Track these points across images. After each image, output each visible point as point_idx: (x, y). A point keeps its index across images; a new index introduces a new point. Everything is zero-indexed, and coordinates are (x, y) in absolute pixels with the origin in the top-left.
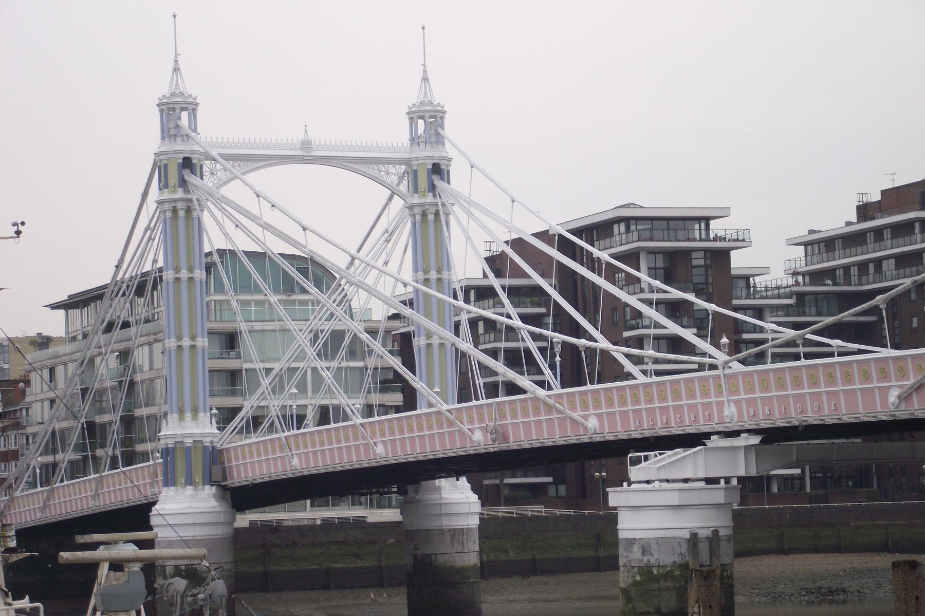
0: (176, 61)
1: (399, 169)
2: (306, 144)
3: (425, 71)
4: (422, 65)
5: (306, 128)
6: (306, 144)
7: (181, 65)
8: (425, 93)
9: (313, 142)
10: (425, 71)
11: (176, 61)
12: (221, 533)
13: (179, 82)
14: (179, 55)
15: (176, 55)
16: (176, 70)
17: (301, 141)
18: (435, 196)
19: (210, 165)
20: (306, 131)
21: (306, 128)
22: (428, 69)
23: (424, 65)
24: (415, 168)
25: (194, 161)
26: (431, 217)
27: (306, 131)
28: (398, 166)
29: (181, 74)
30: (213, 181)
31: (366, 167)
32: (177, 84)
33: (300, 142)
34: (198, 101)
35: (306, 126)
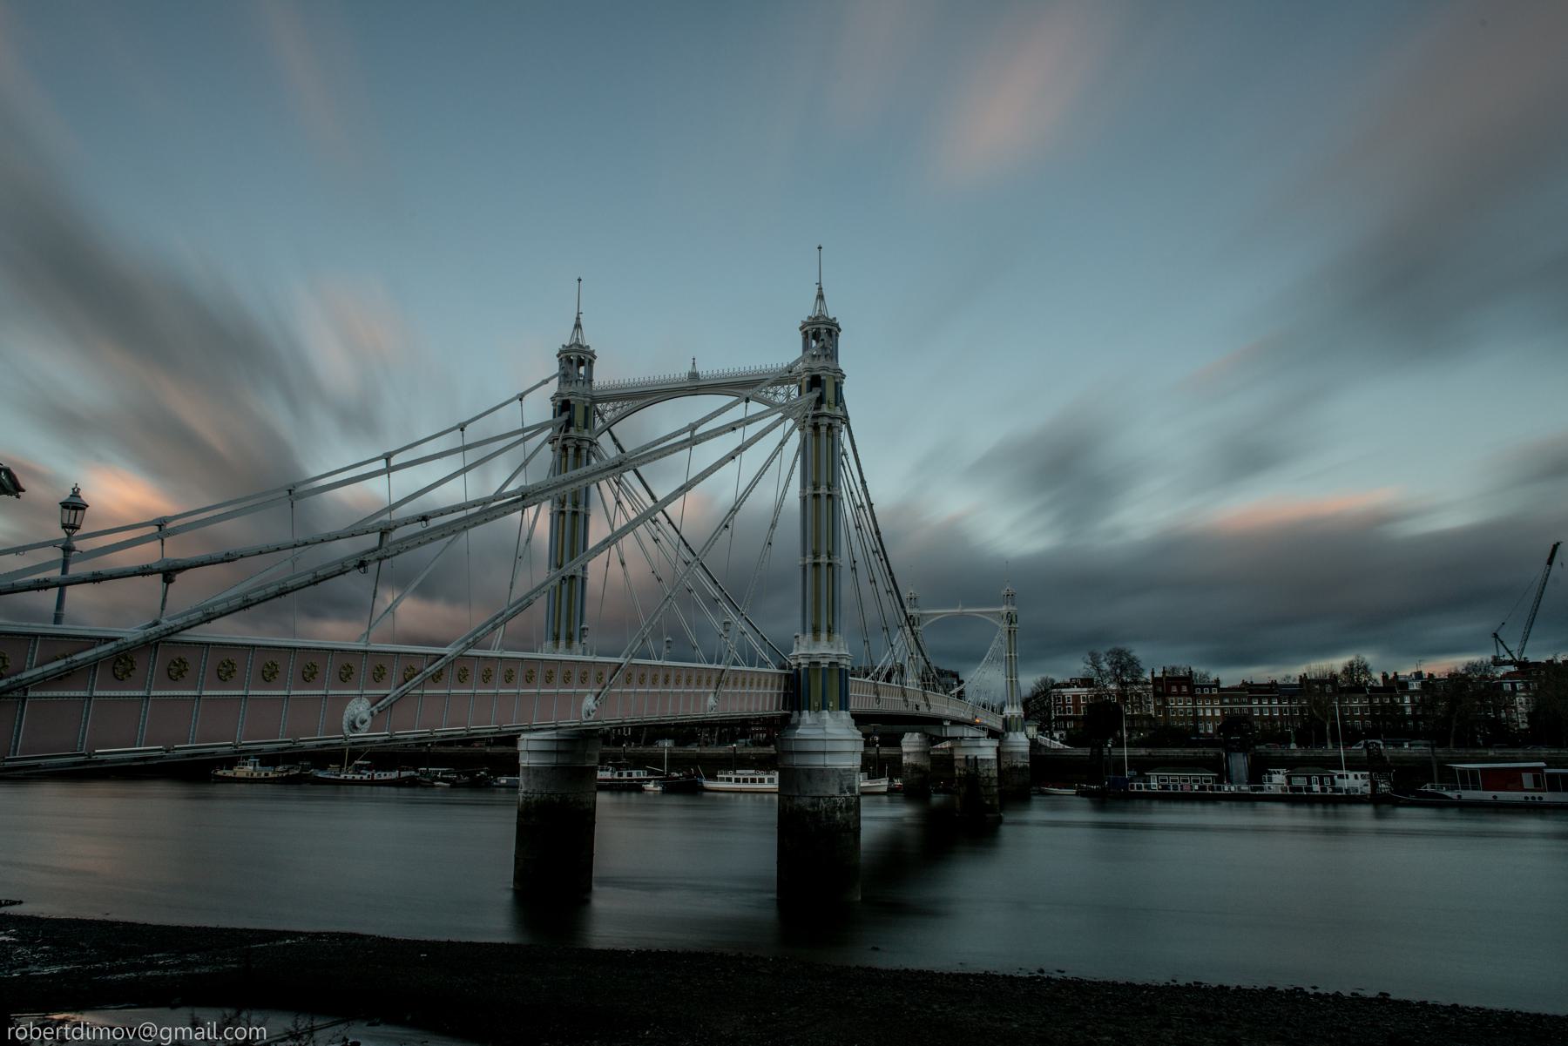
0: (578, 318)
2: (694, 376)
3: (820, 289)
6: (694, 376)
7: (582, 322)
9: (700, 373)
10: (820, 289)
11: (578, 318)
12: (554, 761)
13: (580, 337)
15: (578, 313)
16: (578, 326)
17: (689, 374)
20: (694, 364)
22: (823, 286)
23: (820, 283)
24: (799, 383)
25: (572, 402)
27: (694, 364)
29: (582, 332)
32: (578, 339)
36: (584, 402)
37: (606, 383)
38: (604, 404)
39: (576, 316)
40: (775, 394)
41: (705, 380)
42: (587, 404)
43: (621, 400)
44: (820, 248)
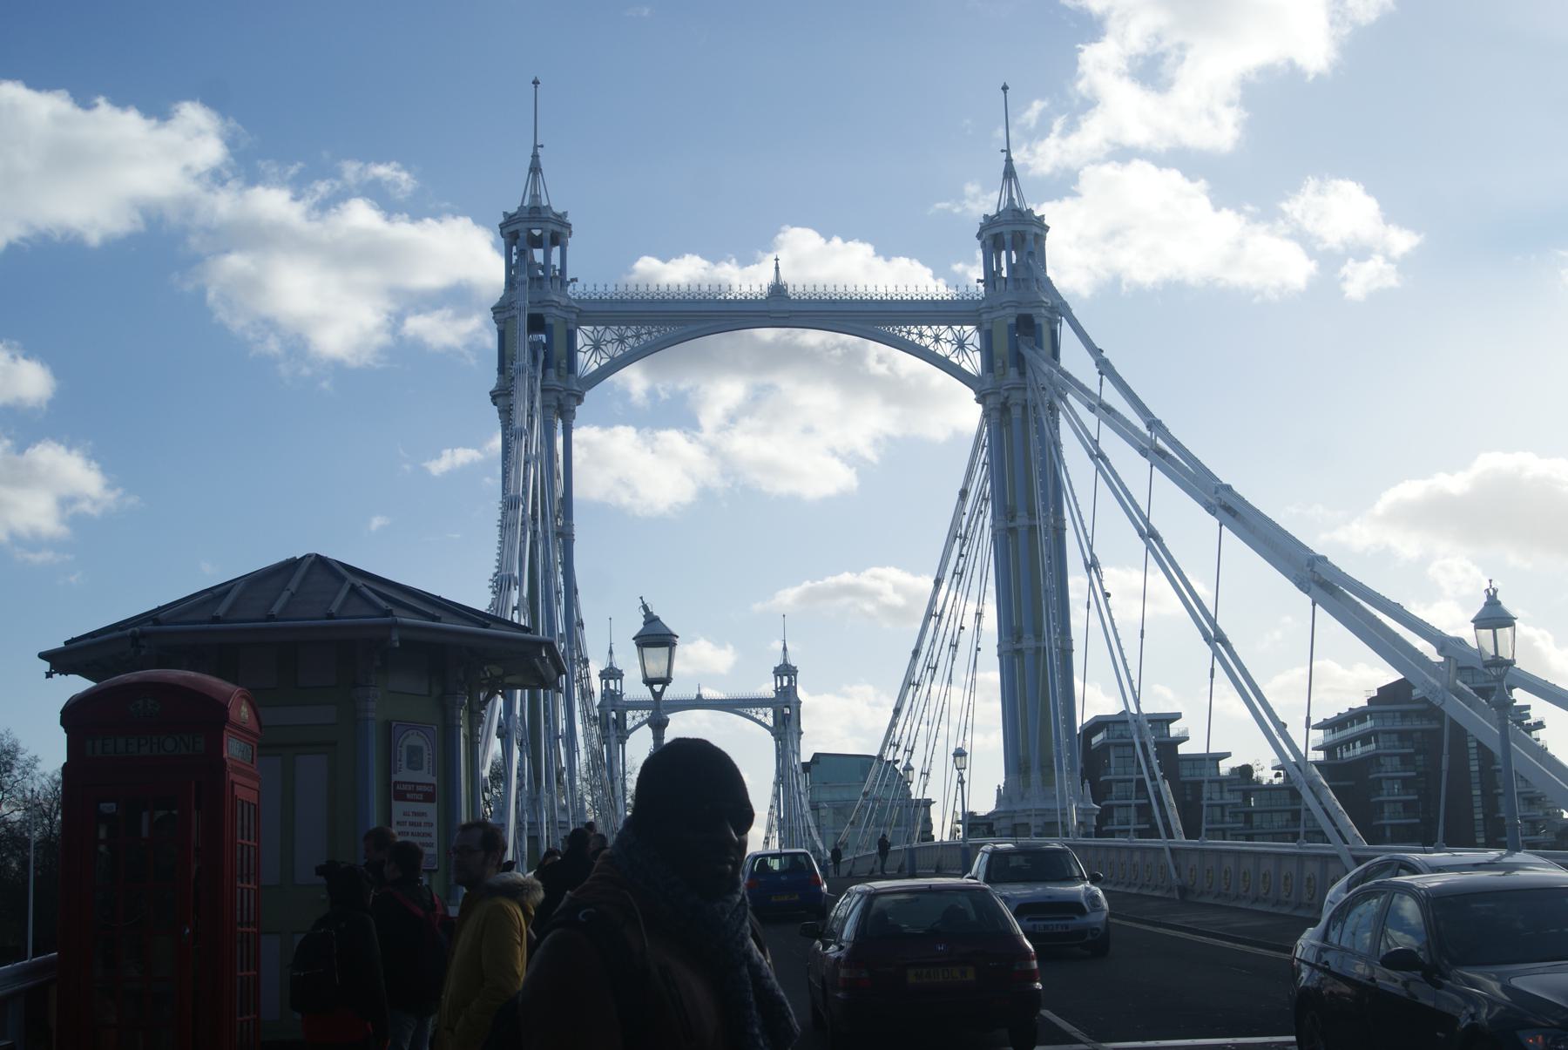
0: (535, 156)
1: (959, 331)
4: (1002, 151)
5: (777, 264)
6: (778, 290)
8: (1011, 199)
9: (790, 290)
14: (542, 146)
15: (536, 147)
18: (1022, 374)
19: (593, 332)
20: (777, 268)
21: (777, 264)
24: (987, 326)
26: (1016, 413)
27: (777, 268)
31: (894, 330)
33: (765, 289)
34: (569, 219)
36: (566, 321)
37: (588, 289)
38: (599, 328)
39: (531, 152)
40: (937, 339)
41: (800, 301)
42: (572, 326)
43: (636, 323)
44: (1005, 88)
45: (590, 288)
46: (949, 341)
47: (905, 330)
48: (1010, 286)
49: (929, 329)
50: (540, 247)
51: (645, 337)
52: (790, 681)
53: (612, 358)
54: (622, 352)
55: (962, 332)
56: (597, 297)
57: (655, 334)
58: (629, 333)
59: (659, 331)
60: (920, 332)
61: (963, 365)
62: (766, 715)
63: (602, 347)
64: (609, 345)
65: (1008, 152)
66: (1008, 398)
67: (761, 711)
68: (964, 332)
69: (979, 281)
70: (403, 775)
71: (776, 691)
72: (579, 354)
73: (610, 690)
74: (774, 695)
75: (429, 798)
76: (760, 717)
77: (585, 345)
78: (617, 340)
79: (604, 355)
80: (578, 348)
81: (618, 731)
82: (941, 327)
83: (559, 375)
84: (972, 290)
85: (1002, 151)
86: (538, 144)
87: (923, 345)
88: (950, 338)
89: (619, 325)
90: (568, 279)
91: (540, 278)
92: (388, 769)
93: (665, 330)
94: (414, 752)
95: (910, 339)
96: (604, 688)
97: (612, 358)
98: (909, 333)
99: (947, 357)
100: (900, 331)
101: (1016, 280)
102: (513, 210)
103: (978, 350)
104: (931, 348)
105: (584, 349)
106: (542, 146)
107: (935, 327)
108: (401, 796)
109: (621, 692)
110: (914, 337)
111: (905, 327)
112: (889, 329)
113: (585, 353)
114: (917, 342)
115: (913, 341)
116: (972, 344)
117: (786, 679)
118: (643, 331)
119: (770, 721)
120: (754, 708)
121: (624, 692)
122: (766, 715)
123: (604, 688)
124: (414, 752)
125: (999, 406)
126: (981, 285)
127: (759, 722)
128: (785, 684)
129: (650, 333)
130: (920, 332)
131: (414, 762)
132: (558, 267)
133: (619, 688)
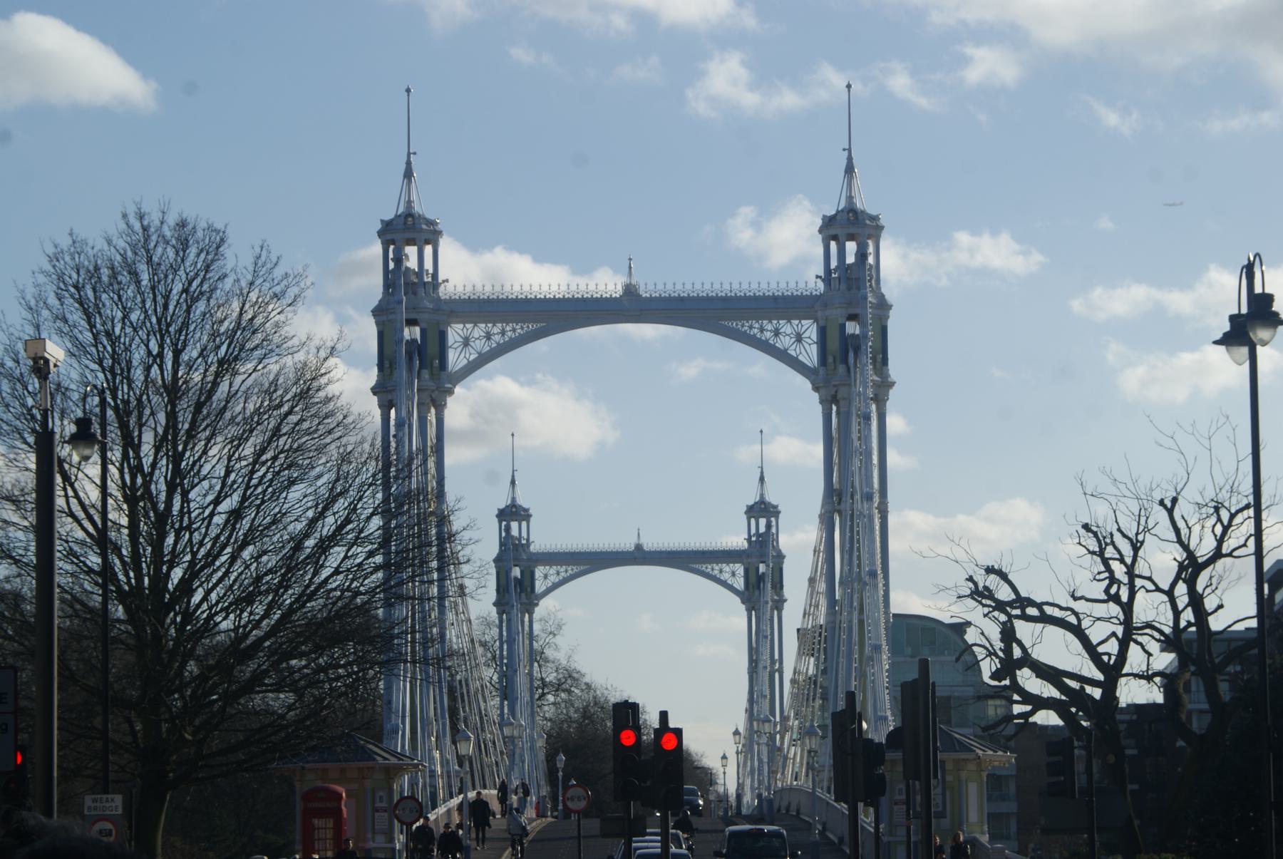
4: (844, 150)
14: (415, 153)
24: (822, 323)
28: (796, 322)
30: (467, 356)
31: (737, 325)
35: (630, 259)
45: (460, 289)
46: (789, 335)
47: (747, 324)
48: (843, 287)
49: (770, 324)
50: (414, 245)
51: (509, 334)
52: (769, 526)
53: (480, 354)
54: (488, 348)
55: (800, 326)
56: (467, 298)
57: (519, 331)
58: (496, 330)
59: (522, 328)
60: (761, 326)
61: (801, 358)
62: (733, 574)
63: (472, 344)
64: (478, 341)
65: (850, 150)
66: (836, 392)
67: (726, 568)
68: (802, 326)
69: (817, 277)
70: (378, 805)
71: (749, 540)
72: (450, 350)
73: (513, 537)
74: (746, 545)
75: (385, 811)
76: (726, 576)
77: (456, 342)
78: (485, 337)
79: (472, 351)
80: (450, 345)
81: (523, 595)
82: (781, 322)
83: (431, 374)
84: (811, 285)
85: (844, 150)
86: (411, 151)
87: (763, 338)
88: (789, 331)
89: (486, 323)
90: (440, 281)
91: (414, 284)
92: (374, 802)
93: (528, 327)
94: (381, 797)
95: (752, 333)
96: (504, 534)
97: (480, 354)
98: (751, 327)
99: (786, 350)
100: (743, 326)
101: (849, 279)
102: (389, 216)
103: (817, 343)
104: (771, 342)
105: (455, 346)
106: (415, 153)
107: (775, 322)
108: (377, 811)
109: (528, 540)
110: (756, 331)
111: (748, 322)
112: (732, 324)
113: (456, 349)
114: (758, 336)
115: (755, 335)
116: (809, 337)
117: (763, 522)
118: (508, 328)
119: (739, 583)
120: (717, 564)
121: (531, 540)
122: (733, 574)
123: (504, 534)
124: (381, 797)
125: (830, 398)
126: (819, 280)
127: (724, 584)
128: (762, 529)
129: (514, 330)
130: (761, 326)
131: (381, 801)
132: (431, 271)
133: (524, 534)
